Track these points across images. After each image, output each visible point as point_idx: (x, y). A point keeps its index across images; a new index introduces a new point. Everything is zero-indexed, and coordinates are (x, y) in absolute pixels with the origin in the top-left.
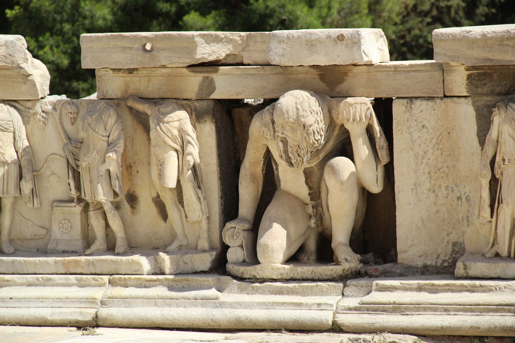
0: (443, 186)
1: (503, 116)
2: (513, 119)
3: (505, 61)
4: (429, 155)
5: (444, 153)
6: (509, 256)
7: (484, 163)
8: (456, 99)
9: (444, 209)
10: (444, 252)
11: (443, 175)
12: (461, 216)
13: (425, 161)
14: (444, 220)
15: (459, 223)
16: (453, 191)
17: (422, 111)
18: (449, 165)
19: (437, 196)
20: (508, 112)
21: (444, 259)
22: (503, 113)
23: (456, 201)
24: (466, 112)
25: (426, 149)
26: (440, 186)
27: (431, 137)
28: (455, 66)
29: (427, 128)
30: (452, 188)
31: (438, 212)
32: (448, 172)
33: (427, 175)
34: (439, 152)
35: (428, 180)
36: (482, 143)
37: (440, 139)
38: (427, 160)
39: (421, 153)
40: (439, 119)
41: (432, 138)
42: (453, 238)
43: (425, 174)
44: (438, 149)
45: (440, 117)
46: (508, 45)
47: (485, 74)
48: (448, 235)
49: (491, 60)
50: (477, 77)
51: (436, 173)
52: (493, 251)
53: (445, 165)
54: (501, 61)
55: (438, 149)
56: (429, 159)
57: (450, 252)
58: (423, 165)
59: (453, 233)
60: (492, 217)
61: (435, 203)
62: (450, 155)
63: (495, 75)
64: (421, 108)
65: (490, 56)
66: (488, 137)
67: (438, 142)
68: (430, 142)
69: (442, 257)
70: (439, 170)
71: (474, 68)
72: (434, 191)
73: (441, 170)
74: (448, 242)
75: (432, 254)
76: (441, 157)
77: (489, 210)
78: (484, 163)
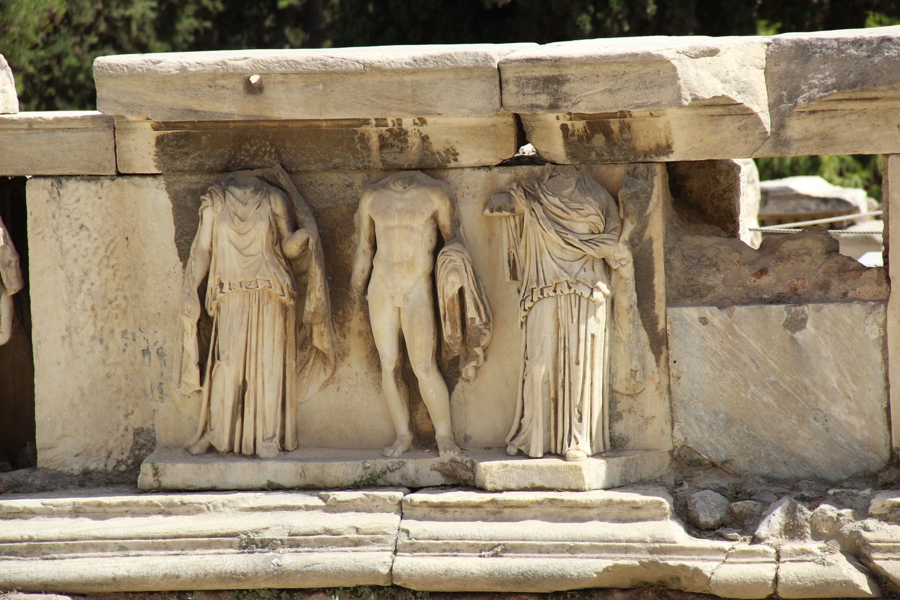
0: (117, 331)
1: (219, 210)
3: (221, 113)
4: (93, 276)
5: (118, 274)
6: (231, 450)
7: (188, 290)
8: (137, 179)
9: (120, 372)
10: (120, 446)
11: (116, 311)
12: (148, 383)
13: (85, 287)
14: (119, 391)
15: (146, 395)
16: (134, 340)
17: (78, 201)
18: (128, 295)
19: (107, 348)
20: (228, 202)
21: (120, 459)
22: (219, 203)
23: (139, 357)
24: (155, 203)
25: (88, 265)
26: (112, 332)
27: (95, 245)
28: (135, 122)
29: (88, 229)
30: (134, 335)
31: (108, 376)
32: (127, 307)
33: (89, 313)
34: (111, 271)
35: (91, 322)
36: (184, 255)
37: (111, 248)
38: (89, 287)
39: (77, 274)
40: (108, 214)
41: (98, 248)
42: (135, 421)
43: (86, 310)
44: (107, 266)
45: (110, 210)
46: (224, 87)
47: (186, 136)
48: (126, 416)
49: (197, 112)
50: (173, 140)
51: (105, 308)
52: (204, 442)
53: (120, 294)
54: (214, 113)
55: (107, 266)
56: (92, 284)
57: (129, 447)
58: (82, 295)
59: (135, 413)
60: (202, 384)
61: (104, 362)
62: (129, 276)
63: (204, 138)
64: (77, 194)
65: (194, 104)
66: (194, 245)
67: (108, 254)
68: (94, 254)
69: (116, 456)
70: (110, 303)
71: (167, 125)
72: (101, 341)
73: (114, 304)
74: (127, 430)
75: (98, 451)
76: (114, 280)
77: (196, 372)
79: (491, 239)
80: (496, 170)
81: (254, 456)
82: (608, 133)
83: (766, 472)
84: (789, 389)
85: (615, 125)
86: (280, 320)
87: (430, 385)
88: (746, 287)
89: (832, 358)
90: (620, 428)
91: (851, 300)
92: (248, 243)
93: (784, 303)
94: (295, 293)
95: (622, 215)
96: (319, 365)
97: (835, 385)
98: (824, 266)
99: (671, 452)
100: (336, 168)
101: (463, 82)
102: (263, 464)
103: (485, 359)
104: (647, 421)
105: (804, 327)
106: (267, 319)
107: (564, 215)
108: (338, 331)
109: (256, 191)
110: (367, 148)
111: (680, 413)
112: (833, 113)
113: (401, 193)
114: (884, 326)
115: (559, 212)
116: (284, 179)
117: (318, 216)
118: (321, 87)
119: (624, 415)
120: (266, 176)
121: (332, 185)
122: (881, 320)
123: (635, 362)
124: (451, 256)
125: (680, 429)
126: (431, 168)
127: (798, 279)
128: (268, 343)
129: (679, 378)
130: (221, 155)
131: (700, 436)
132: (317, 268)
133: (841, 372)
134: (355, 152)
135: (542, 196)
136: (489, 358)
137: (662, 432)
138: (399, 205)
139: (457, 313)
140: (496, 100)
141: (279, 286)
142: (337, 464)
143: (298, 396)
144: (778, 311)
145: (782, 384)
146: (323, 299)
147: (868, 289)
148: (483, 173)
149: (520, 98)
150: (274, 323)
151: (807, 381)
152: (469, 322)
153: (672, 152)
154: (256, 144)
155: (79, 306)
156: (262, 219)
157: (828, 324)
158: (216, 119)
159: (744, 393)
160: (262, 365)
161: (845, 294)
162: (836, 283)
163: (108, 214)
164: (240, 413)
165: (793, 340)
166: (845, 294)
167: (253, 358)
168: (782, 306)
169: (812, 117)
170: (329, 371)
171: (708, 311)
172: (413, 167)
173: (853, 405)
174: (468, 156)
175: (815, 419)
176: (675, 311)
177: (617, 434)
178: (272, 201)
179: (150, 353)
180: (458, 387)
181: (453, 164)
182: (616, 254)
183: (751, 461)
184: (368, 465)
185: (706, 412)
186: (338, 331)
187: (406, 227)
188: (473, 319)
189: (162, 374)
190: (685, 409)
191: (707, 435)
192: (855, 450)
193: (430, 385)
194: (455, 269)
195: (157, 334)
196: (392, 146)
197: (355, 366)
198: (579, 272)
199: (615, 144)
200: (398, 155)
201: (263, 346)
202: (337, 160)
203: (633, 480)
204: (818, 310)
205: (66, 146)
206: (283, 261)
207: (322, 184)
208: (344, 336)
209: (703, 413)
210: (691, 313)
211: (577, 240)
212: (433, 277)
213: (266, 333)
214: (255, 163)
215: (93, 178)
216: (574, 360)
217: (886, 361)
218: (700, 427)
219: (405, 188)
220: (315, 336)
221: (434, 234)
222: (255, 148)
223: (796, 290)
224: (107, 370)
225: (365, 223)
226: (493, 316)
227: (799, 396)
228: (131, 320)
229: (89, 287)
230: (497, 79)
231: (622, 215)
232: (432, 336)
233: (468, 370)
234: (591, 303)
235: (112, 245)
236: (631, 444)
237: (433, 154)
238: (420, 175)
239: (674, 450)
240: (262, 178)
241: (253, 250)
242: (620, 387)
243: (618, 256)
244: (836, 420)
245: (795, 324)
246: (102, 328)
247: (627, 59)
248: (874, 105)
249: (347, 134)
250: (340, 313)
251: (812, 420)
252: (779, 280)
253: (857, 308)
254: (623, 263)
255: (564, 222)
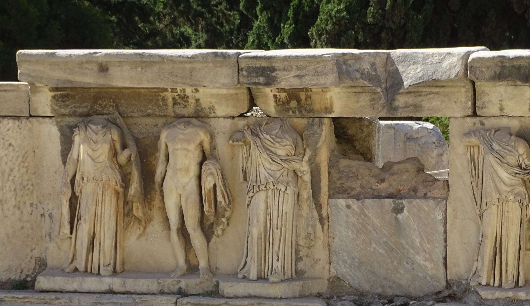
0: (28, 203)
1: (83, 137)
2: (91, 139)
3: (85, 83)
4: (15, 172)
5: (29, 171)
6: (86, 271)
7: (65, 181)
8: (41, 119)
9: (28, 226)
10: (28, 266)
11: (28, 192)
12: (44, 233)
13: (11, 178)
14: (28, 236)
15: (42, 239)
16: (37, 208)
17: (8, 130)
18: (34, 183)
19: (22, 212)
20: (88, 132)
21: (28, 274)
22: (83, 133)
23: (39, 218)
24: (50, 132)
25: (13, 166)
26: (25, 203)
27: (17, 155)
28: (40, 87)
29: (13, 146)
30: (36, 205)
31: (22, 228)
32: (33, 190)
33: (12, 193)
34: (25, 170)
35: (14, 197)
36: (64, 162)
37: (25, 157)
38: (13, 178)
39: (7, 170)
40: (25, 137)
41: (18, 157)
42: (36, 253)
43: (11, 191)
44: (23, 167)
45: (25, 135)
46: (87, 68)
47: (67, 96)
48: (32, 250)
49: (71, 82)
50: (60, 98)
51: (21, 190)
52: (72, 266)
53: (30, 182)
54: (81, 83)
55: (23, 167)
56: (15, 177)
57: (33, 268)
58: (9, 183)
59: (36, 249)
60: (71, 233)
61: (20, 220)
62: (35, 173)
63: (77, 97)
64: (8, 127)
65: (70, 78)
66: (69, 156)
67: (24, 160)
68: (17, 160)
69: (25, 272)
70: (24, 187)
71: (56, 89)
72: (19, 208)
73: (26, 188)
74: (32, 258)
75: (16, 269)
76: (27, 174)
77: (68, 227)
78: (65, 181)
79: (233, 157)
80: (237, 119)
81: (99, 274)
82: (299, 101)
83: (380, 292)
84: (393, 246)
85: (303, 96)
86: (114, 200)
87: (197, 238)
88: (373, 189)
89: (417, 229)
90: (301, 265)
91: (429, 198)
92: (98, 155)
93: (393, 198)
94: (124, 185)
95: (305, 146)
96: (136, 225)
97: (418, 244)
98: (415, 179)
99: (329, 280)
100: (149, 115)
101: (218, 69)
102: (103, 279)
103: (228, 224)
104: (316, 261)
105: (403, 212)
106: (107, 199)
107: (272, 145)
108: (147, 207)
109: (104, 127)
110: (166, 105)
111: (334, 258)
112: (421, 94)
113: (183, 130)
114: (445, 212)
115: (269, 143)
116: (120, 120)
117: (137, 141)
118: (140, 69)
119: (304, 258)
120: (110, 119)
121: (146, 125)
122: (444, 209)
123: (310, 229)
124: (209, 167)
125: (334, 267)
126: (200, 117)
127: (401, 185)
128: (107, 212)
129: (334, 238)
130: (86, 107)
131: (344, 270)
132: (136, 171)
133: (421, 237)
134: (159, 107)
135: (260, 134)
136: (230, 224)
137: (324, 268)
138: (182, 137)
139: (212, 198)
140: (236, 79)
141: (114, 180)
142: (143, 280)
143: (124, 242)
144: (389, 202)
145: (389, 243)
146: (139, 188)
147: (438, 192)
148: (229, 120)
149: (249, 79)
150: (111, 201)
151: (403, 242)
152: (218, 203)
153: (334, 112)
154: (105, 101)
155: (7, 188)
156: (106, 142)
157: (415, 210)
158: (82, 86)
159: (369, 247)
160: (104, 224)
161: (425, 194)
162: (421, 188)
163: (25, 137)
164: (91, 251)
165: (396, 219)
166: (425, 194)
167: (99, 220)
168: (391, 200)
169: (409, 95)
170: (142, 229)
171: (350, 202)
172: (191, 116)
173: (427, 256)
174: (221, 111)
175: (407, 263)
176: (332, 201)
177: (299, 269)
178: (112, 132)
179: (45, 216)
180: (214, 239)
181: (213, 115)
182: (300, 168)
183: (371, 286)
184: (160, 281)
185: (348, 258)
186: (147, 207)
187: (185, 149)
188: (221, 202)
189: (51, 228)
190: (337, 256)
191: (348, 270)
192: (427, 280)
193: (197, 238)
194: (212, 174)
195: (49, 205)
196: (180, 104)
197: (156, 226)
198: (279, 178)
199: (303, 107)
200: (183, 109)
201: (104, 213)
202: (149, 111)
203: (307, 294)
204: (410, 203)
205: (3, 100)
206: (117, 166)
207: (141, 124)
208: (151, 210)
209: (346, 258)
210: (342, 202)
211: (279, 159)
212: (199, 178)
213: (106, 206)
214: (105, 111)
215: (17, 118)
216: (275, 226)
217: (445, 232)
218: (344, 266)
219: (185, 127)
220: (134, 209)
221: (201, 154)
222: (105, 103)
223: (400, 191)
224: (21, 225)
225: (163, 146)
226: (233, 201)
227: (399, 249)
228: (35, 198)
229: (13, 178)
230: (237, 67)
231: (305, 146)
232: (198, 211)
233: (218, 230)
234: (286, 195)
235: (26, 155)
236: (307, 275)
237: (202, 109)
238: (194, 120)
239: (330, 278)
240: (108, 120)
241: (100, 160)
242: (301, 242)
243: (302, 169)
244: (418, 264)
245: (398, 210)
246: (20, 201)
247: (308, 59)
248: (442, 90)
249: (154, 96)
250: (149, 196)
251: (405, 263)
252: (390, 185)
253: (431, 202)
254: (305, 173)
255: (272, 149)
